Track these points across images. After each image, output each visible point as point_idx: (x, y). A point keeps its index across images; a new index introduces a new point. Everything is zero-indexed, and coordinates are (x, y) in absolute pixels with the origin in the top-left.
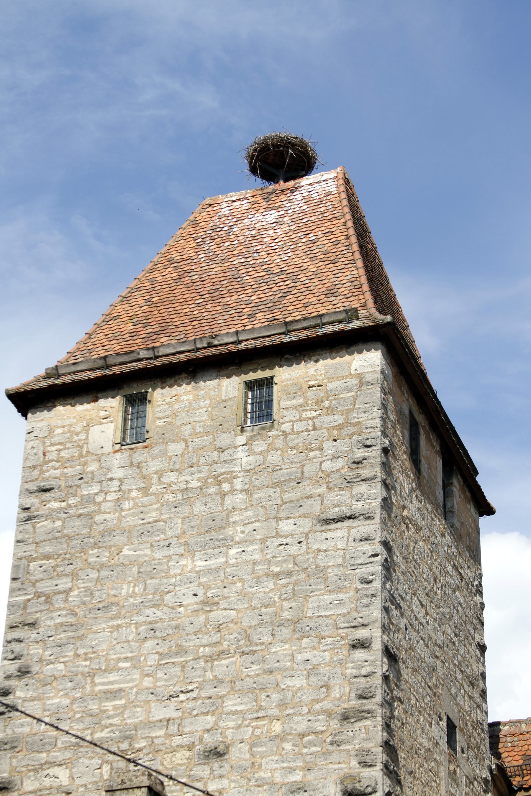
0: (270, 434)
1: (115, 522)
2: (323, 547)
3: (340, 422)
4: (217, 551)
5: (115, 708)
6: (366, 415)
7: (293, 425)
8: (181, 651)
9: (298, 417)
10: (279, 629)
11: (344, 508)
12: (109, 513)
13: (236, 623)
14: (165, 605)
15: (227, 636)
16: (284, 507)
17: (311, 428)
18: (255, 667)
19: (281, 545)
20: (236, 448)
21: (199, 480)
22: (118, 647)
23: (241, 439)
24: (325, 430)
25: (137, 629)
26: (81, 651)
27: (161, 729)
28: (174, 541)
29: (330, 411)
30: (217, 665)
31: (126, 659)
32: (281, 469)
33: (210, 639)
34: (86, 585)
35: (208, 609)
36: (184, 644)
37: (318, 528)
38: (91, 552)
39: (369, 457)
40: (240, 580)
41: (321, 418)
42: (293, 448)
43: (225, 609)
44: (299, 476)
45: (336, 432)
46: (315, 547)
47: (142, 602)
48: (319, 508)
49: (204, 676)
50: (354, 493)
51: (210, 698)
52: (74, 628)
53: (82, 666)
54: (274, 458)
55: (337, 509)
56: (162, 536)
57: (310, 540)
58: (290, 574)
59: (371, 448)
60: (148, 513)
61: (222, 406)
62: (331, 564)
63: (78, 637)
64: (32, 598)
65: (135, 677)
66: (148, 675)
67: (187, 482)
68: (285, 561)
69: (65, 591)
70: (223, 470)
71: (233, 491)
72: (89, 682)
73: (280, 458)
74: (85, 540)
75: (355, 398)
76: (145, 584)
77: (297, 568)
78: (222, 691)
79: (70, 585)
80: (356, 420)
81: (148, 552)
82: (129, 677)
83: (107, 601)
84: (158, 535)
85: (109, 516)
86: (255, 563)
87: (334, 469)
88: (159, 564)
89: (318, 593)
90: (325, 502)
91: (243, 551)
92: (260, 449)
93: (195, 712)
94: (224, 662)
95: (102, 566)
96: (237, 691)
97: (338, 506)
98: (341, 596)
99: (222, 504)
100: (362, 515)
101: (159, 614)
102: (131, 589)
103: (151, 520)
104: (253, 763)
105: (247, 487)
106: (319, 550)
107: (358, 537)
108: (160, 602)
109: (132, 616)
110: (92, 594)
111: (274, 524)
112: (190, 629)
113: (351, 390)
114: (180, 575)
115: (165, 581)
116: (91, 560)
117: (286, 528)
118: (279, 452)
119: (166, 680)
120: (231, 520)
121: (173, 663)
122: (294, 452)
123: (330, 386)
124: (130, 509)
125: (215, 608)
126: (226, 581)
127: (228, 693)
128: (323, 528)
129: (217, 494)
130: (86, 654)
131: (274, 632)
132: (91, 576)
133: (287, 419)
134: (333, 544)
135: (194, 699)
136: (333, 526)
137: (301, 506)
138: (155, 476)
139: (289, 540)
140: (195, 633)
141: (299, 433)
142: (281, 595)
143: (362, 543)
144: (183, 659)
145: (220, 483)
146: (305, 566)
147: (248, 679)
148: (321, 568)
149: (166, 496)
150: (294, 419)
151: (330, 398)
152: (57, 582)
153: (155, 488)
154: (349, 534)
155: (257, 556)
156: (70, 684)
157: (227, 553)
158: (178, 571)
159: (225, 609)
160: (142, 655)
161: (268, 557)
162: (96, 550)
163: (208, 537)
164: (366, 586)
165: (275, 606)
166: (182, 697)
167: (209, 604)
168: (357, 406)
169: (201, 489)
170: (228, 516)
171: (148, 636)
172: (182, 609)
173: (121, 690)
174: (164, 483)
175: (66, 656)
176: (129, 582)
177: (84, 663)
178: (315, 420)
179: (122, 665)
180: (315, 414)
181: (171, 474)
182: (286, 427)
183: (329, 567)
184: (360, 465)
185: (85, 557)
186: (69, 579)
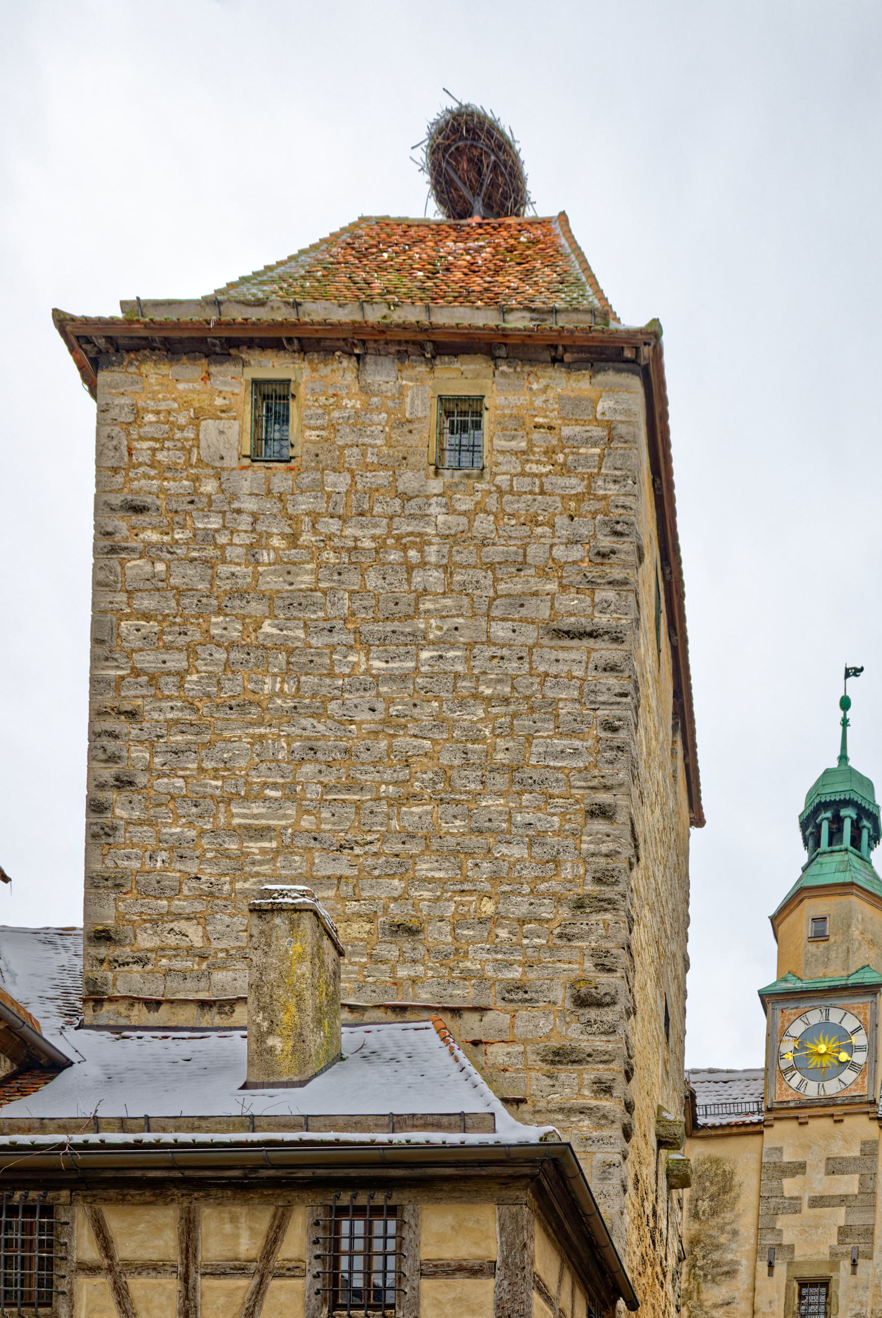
0: (479, 486)
1: (249, 580)
2: (553, 670)
3: (579, 490)
4: (402, 650)
5: (263, 851)
6: (617, 487)
7: (512, 481)
9: (519, 469)
10: (492, 775)
11: (583, 620)
12: (238, 564)
13: (432, 758)
14: (329, 717)
15: (419, 775)
16: (497, 602)
17: (537, 490)
18: (458, 823)
19: (494, 657)
20: (428, 497)
21: (374, 538)
22: (263, 767)
23: (435, 486)
24: (558, 499)
25: (288, 745)
26: (208, 765)
27: (329, 889)
28: (339, 624)
29: (565, 470)
31: (275, 786)
32: (494, 544)
33: (395, 775)
34: (210, 669)
35: (392, 732)
36: (358, 776)
37: (546, 641)
38: (214, 620)
39: (619, 551)
40: (436, 698)
41: (553, 479)
42: (512, 516)
43: (415, 736)
44: (520, 559)
45: (573, 504)
46: (541, 669)
47: (295, 708)
48: (548, 612)
50: (597, 600)
51: (397, 856)
52: (196, 729)
53: (211, 786)
54: (484, 525)
55: (573, 619)
56: (321, 614)
57: (534, 658)
58: (506, 701)
59: (623, 539)
60: (298, 575)
61: (406, 429)
62: (563, 696)
63: (203, 744)
64: (129, 675)
65: (289, 812)
67: (356, 539)
68: (500, 681)
69: (178, 673)
70: (410, 529)
71: (423, 564)
72: (223, 810)
73: (492, 527)
74: (204, 600)
75: (601, 457)
76: (299, 682)
77: (516, 695)
78: (413, 848)
79: (185, 664)
80: (601, 492)
81: (301, 634)
82: (281, 812)
83: (242, 697)
84: (315, 612)
85: (239, 568)
86: (457, 676)
87: (570, 560)
88: (319, 655)
89: (545, 734)
90: (557, 605)
91: (441, 657)
92: (464, 507)
93: (376, 873)
94: (414, 809)
95: (233, 645)
96: (433, 851)
97: (575, 615)
98: (577, 743)
99: (409, 581)
100: (607, 632)
101: (321, 727)
102: (278, 686)
103: (303, 586)
104: (457, 950)
105: (445, 561)
106: (547, 675)
107: (601, 664)
108: (321, 711)
109: (281, 724)
110: (219, 682)
111: (484, 624)
113: (595, 444)
114: (349, 676)
115: (328, 681)
116: (215, 631)
117: (501, 634)
118: (491, 518)
120: (422, 607)
121: (343, 801)
122: (513, 522)
123: (566, 431)
124: (270, 564)
125: (401, 733)
126: (416, 695)
127: (422, 853)
128: (553, 643)
129: (401, 564)
130: (216, 770)
131: (484, 779)
132: (217, 656)
133: (504, 468)
134: (566, 669)
135: (375, 854)
136: (567, 643)
137: (522, 605)
138: (307, 519)
139: (505, 652)
140: (374, 764)
141: (520, 494)
142: (494, 729)
143: (607, 674)
144: (356, 797)
145: (405, 549)
146: (528, 693)
147: (448, 837)
148: (550, 701)
149: (325, 555)
150: (513, 471)
151: (567, 451)
152: (165, 657)
153: (306, 538)
154: (588, 658)
155: (460, 668)
156: (194, 810)
157: (418, 656)
158: (347, 671)
159: (415, 736)
160: (298, 783)
161: (476, 671)
162: (221, 618)
163: (389, 627)
164: (609, 735)
165: (486, 743)
166: (358, 850)
167: (391, 725)
168: (603, 471)
169: (377, 552)
170: (417, 600)
171: (306, 757)
172: (353, 727)
173: (269, 828)
174: (321, 534)
175: (187, 769)
176: (275, 675)
177: (214, 783)
178: (544, 479)
179: (269, 793)
180: (544, 470)
181: (331, 521)
182: (502, 480)
183: (560, 700)
184: (606, 561)
185: (205, 626)
186: (183, 656)
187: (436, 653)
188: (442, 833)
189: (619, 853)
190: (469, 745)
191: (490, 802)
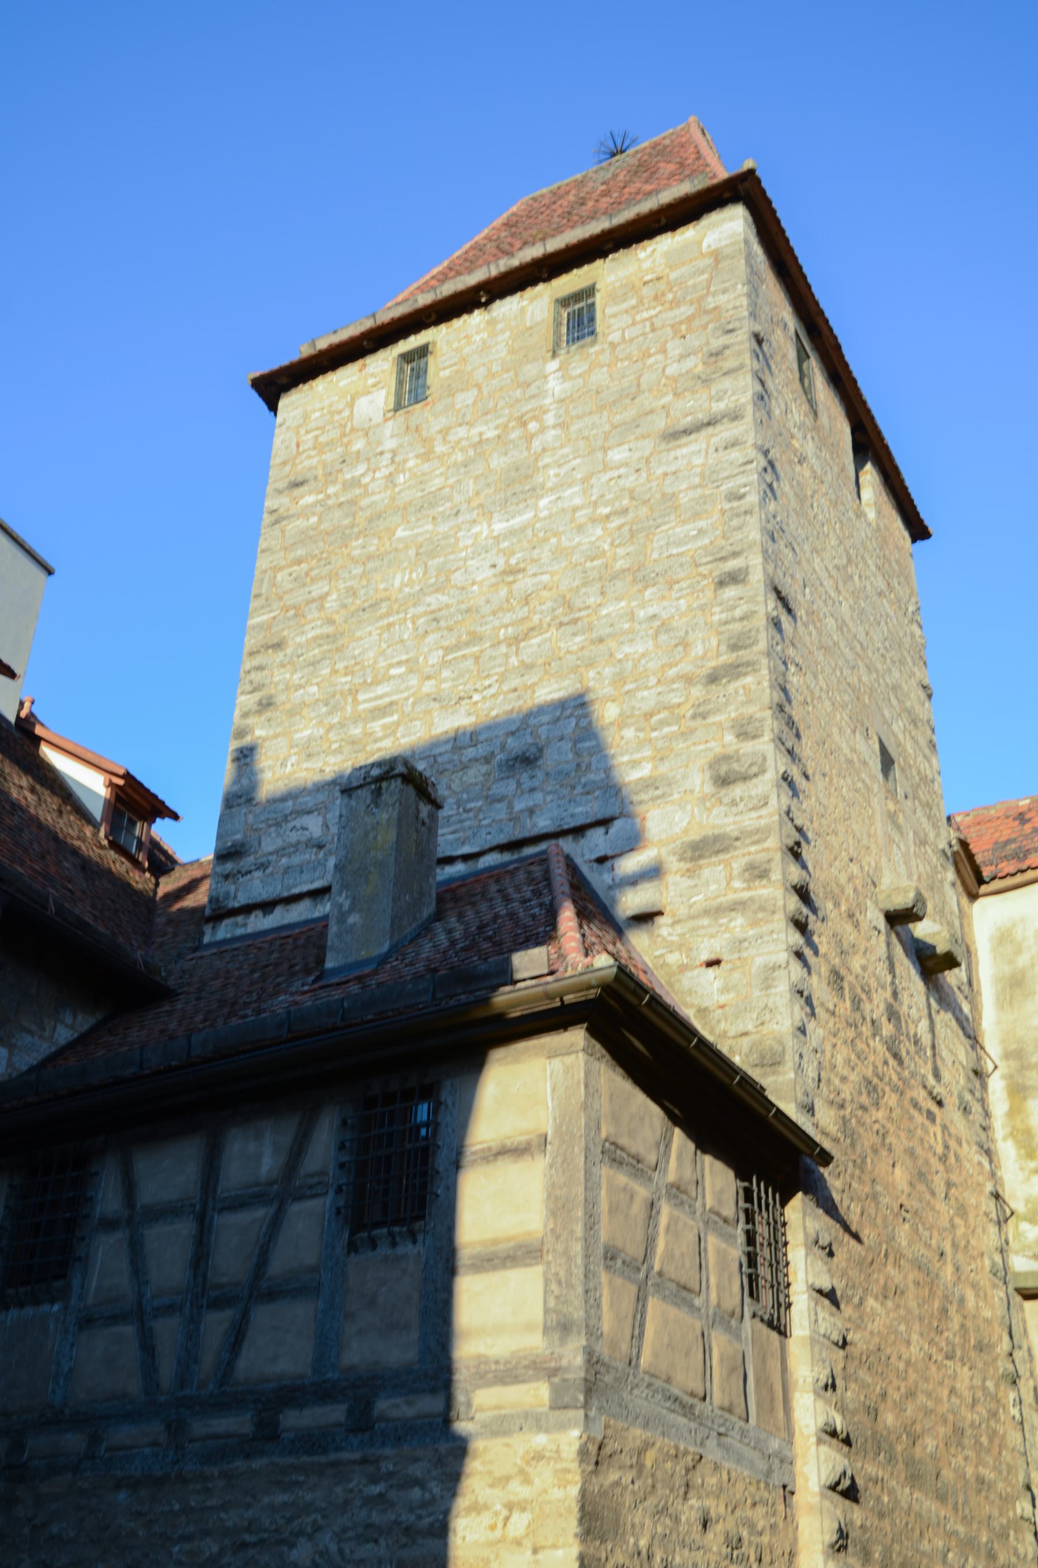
8: (475, 638)
13: (551, 589)
30: (524, 648)
49: (506, 664)
66: (428, 678)
78: (531, 679)
86: (575, 509)
91: (559, 498)
99: (528, 449)
112: (486, 610)
119: (453, 680)
121: (464, 656)
129: (520, 438)
135: (493, 696)
155: (578, 501)
157: (536, 505)
166: (476, 697)
179: (393, 672)
187: (553, 497)
188: (562, 654)
189: (755, 612)
190: (589, 564)
191: (611, 609)
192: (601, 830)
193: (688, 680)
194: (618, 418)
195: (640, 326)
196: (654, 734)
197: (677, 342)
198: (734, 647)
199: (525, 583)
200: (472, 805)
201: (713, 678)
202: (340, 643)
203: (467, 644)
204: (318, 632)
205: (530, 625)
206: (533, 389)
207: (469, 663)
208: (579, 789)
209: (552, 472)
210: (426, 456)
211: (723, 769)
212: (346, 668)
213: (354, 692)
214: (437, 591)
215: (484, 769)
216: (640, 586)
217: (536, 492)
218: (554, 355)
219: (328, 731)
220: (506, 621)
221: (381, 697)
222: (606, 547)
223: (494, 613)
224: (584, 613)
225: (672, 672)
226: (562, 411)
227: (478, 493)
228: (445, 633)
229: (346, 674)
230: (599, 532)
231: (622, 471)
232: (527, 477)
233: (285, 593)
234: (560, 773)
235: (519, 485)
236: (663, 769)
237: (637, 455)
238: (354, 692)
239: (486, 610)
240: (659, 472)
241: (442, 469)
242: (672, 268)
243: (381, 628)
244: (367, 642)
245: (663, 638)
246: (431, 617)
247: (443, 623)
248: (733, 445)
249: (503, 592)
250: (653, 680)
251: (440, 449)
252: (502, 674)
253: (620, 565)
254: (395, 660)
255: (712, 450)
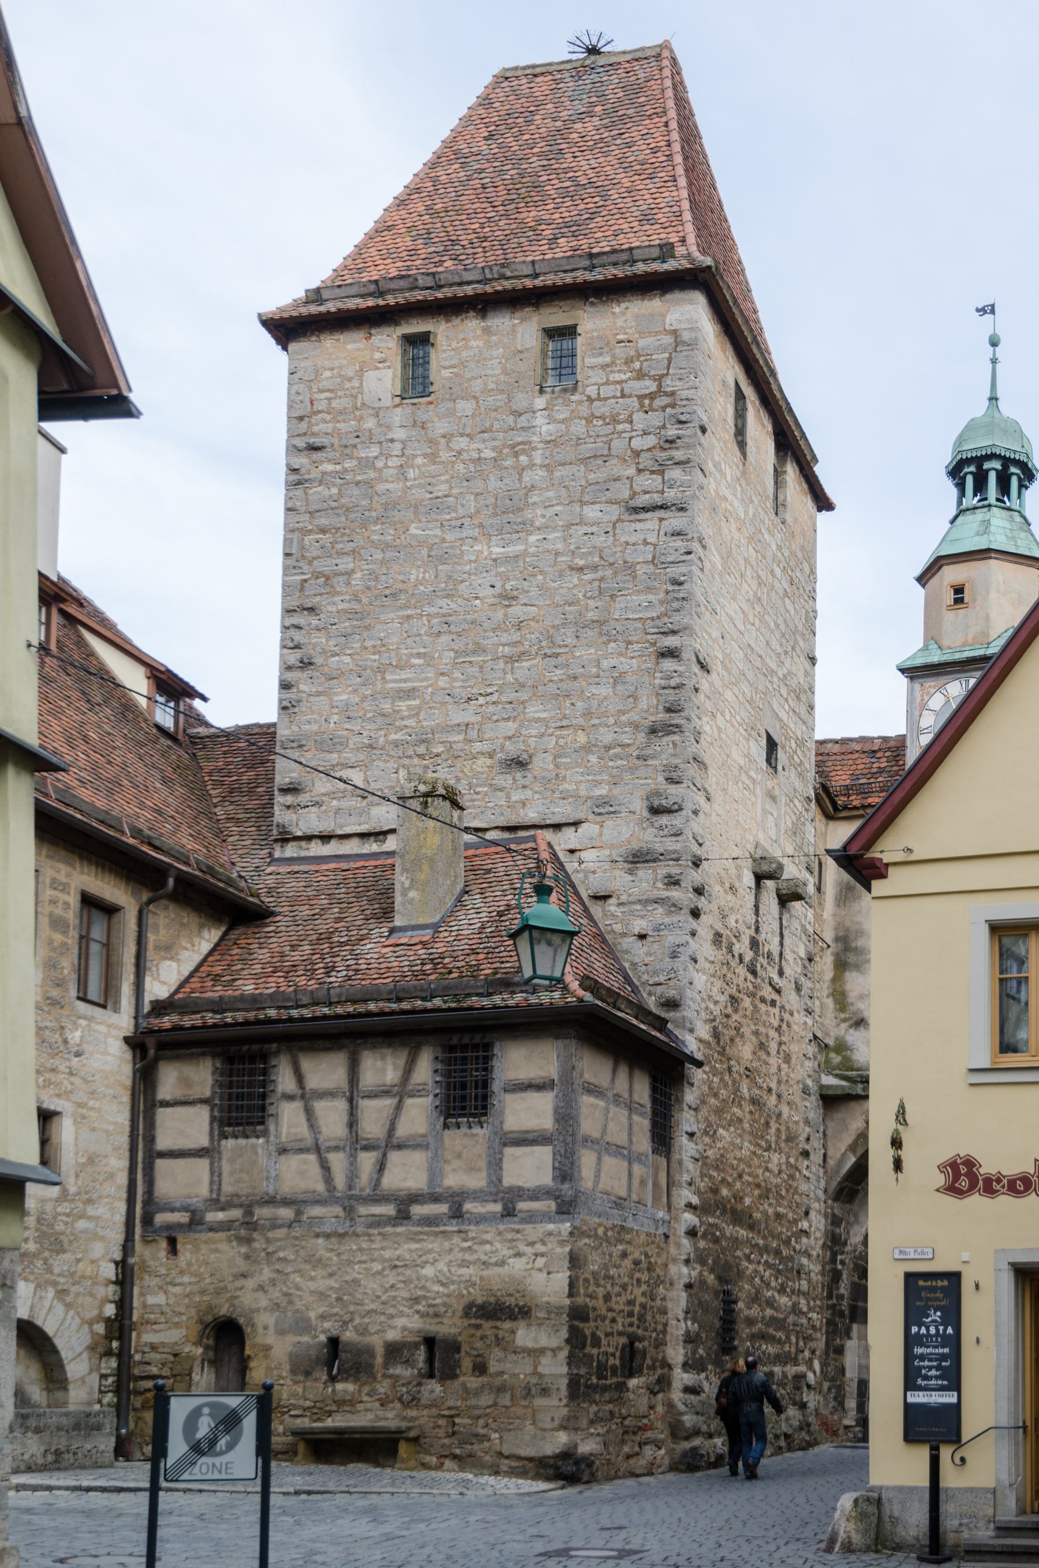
192: (572, 829)
193: (636, 726)
194: (592, 476)
195: (612, 387)
196: (611, 764)
197: (641, 414)
198: (669, 710)
199: (517, 611)
200: (478, 789)
201: (653, 731)
202: (367, 622)
203: (474, 652)
204: (346, 606)
205: (521, 649)
206: (523, 421)
207: (475, 670)
208: (557, 795)
209: (539, 512)
210: (432, 457)
211: (656, 803)
212: (374, 647)
213: (381, 670)
214: (447, 596)
215: (489, 762)
216: (605, 638)
217: (525, 527)
218: (542, 391)
219: (363, 701)
220: (503, 640)
221: (405, 681)
222: (580, 595)
223: (494, 630)
224: (562, 650)
225: (624, 718)
226: (548, 453)
227: (478, 512)
228: (455, 637)
229: (374, 653)
230: (575, 581)
231: (594, 529)
232: (520, 510)
233: (314, 558)
234: (544, 778)
235: (509, 515)
236: (616, 791)
237: (606, 518)
238: (381, 670)
239: (487, 625)
240: (623, 539)
241: (447, 477)
242: (641, 334)
243: (402, 617)
244: (389, 626)
245: (619, 687)
246: (444, 619)
247: (452, 627)
248: (679, 534)
249: (500, 614)
250: (611, 721)
251: (444, 455)
252: (501, 686)
253: (590, 615)
254: (415, 651)
255: (662, 533)
